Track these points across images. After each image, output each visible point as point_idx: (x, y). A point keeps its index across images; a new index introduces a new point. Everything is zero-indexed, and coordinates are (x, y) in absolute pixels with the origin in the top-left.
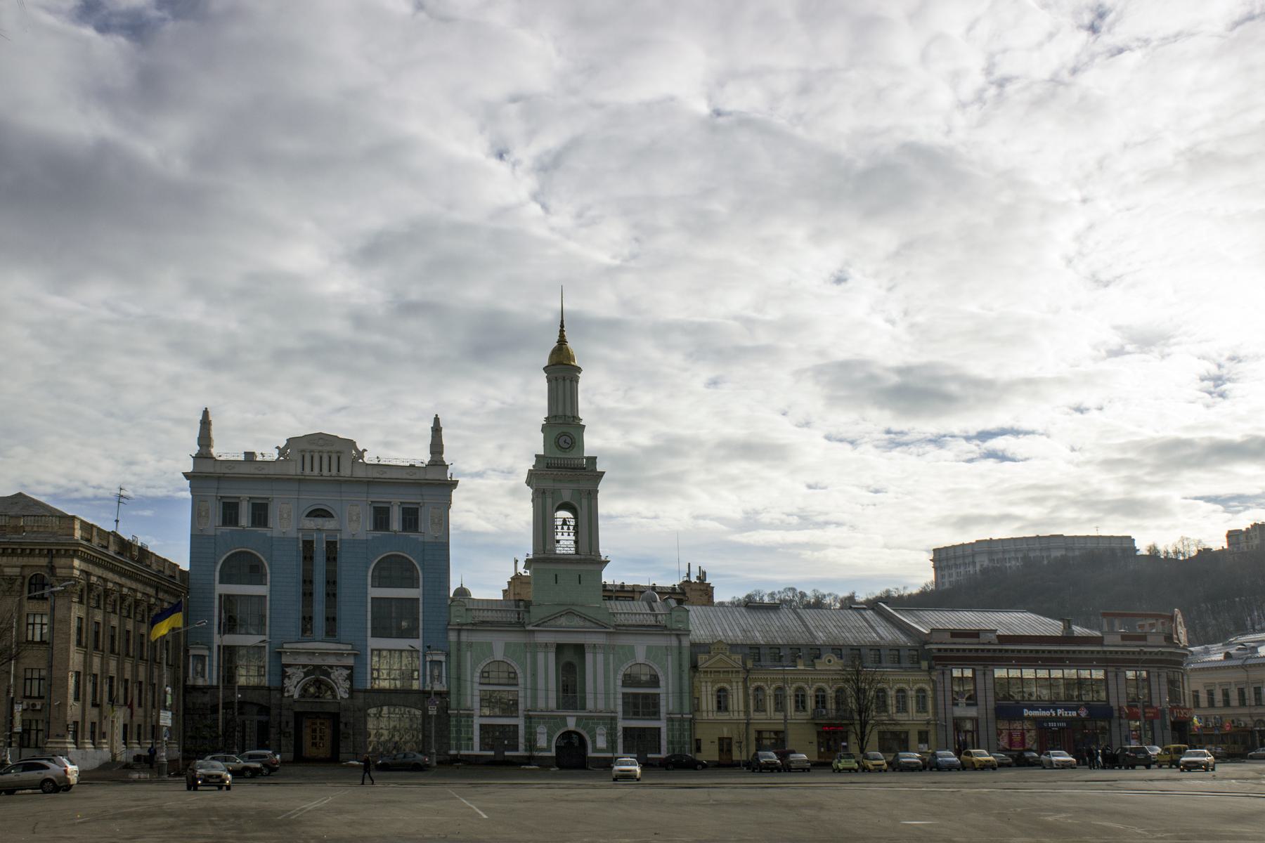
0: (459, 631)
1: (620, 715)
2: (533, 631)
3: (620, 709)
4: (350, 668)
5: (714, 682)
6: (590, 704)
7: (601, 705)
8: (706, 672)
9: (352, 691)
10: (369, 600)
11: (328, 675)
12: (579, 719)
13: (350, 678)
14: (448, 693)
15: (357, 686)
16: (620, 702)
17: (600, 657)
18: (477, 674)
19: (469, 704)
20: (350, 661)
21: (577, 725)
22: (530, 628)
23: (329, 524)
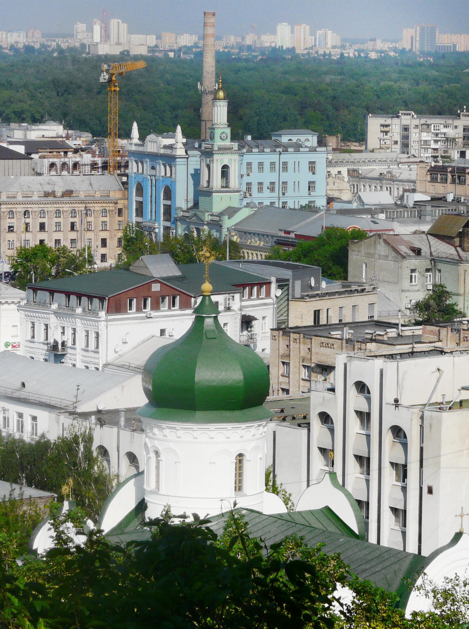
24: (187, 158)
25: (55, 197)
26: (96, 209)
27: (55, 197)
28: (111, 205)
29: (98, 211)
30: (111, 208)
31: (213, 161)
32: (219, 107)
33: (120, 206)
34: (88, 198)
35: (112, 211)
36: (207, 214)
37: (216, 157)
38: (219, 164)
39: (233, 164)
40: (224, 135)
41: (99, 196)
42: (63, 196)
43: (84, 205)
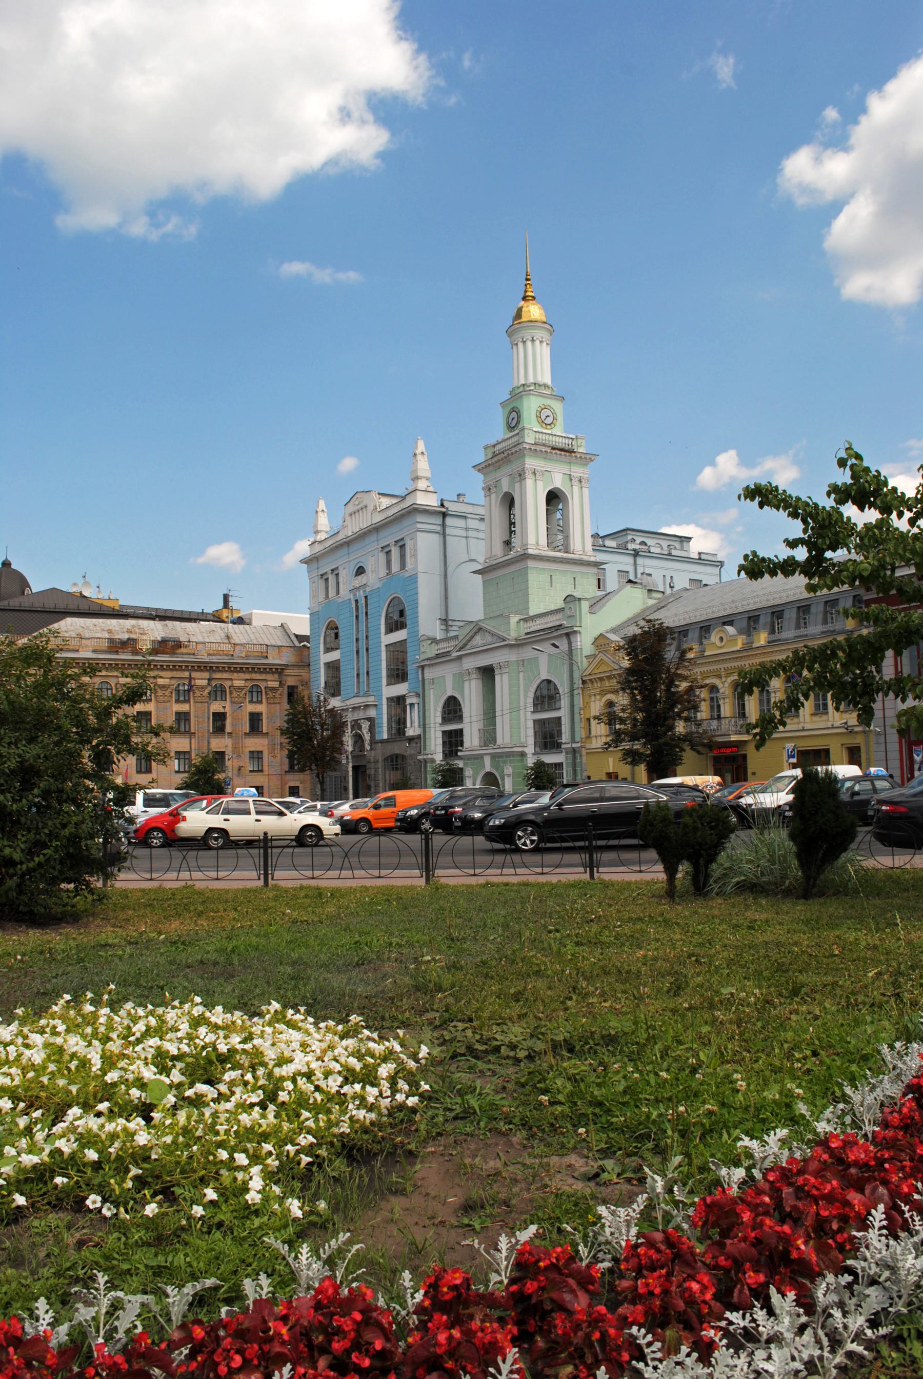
0: (423, 667)
1: (530, 750)
2: (459, 658)
3: (531, 741)
4: (370, 719)
5: (603, 693)
6: (499, 741)
7: (507, 740)
8: (591, 680)
9: (373, 741)
10: (383, 649)
11: (360, 728)
12: (494, 756)
13: (372, 729)
14: (419, 737)
15: (378, 737)
16: (531, 732)
17: (505, 677)
18: (439, 714)
19: (433, 748)
20: (372, 713)
21: (492, 766)
22: (455, 654)
23: (362, 579)
24: (444, 515)
25: (136, 652)
26: (237, 683)
27: (136, 652)
28: (269, 677)
29: (240, 689)
30: (271, 684)
31: (521, 476)
32: (529, 343)
33: (291, 682)
34: (214, 659)
35: (273, 689)
36: (514, 619)
37: (531, 463)
38: (540, 484)
39: (576, 489)
40: (548, 413)
41: (243, 655)
42: (154, 651)
43: (206, 675)
